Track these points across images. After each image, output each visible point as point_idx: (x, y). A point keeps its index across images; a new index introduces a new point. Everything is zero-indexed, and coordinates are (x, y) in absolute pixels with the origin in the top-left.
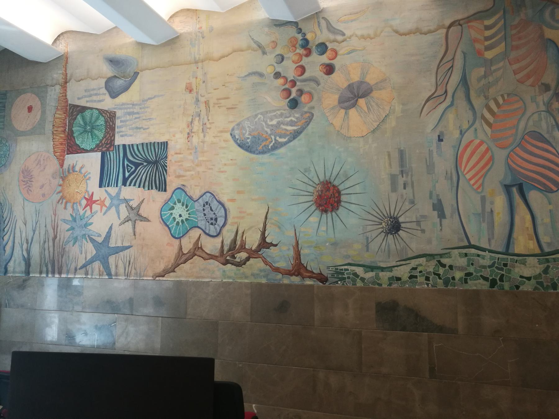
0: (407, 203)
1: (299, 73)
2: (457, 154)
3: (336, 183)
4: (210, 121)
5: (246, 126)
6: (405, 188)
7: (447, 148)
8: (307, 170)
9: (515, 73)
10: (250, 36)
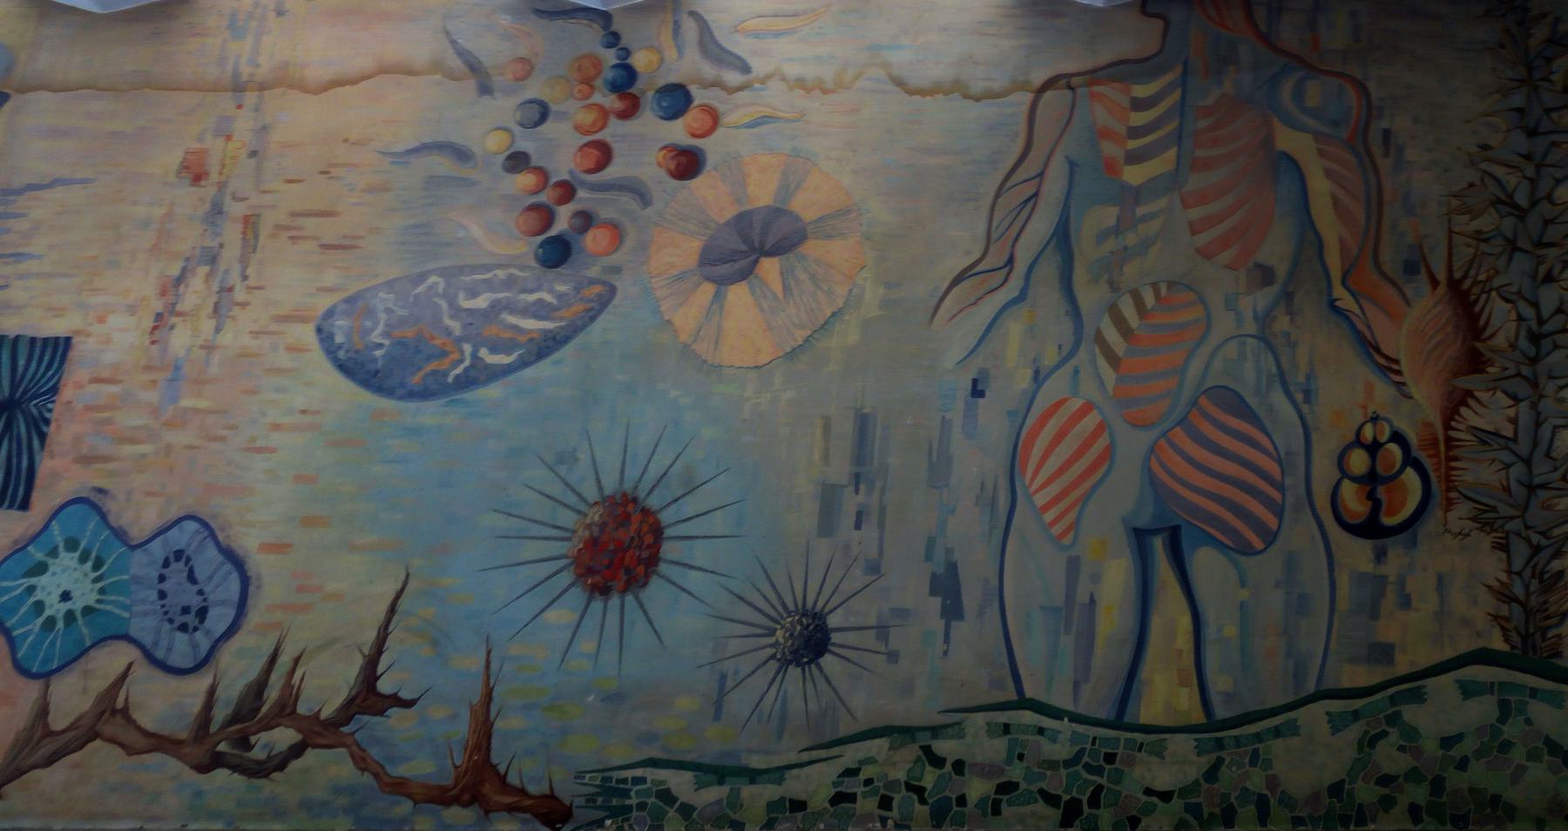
0: (857, 571)
1: (591, 164)
2: (1018, 435)
3: (653, 502)
4: (252, 282)
5: (380, 306)
6: (858, 526)
7: (993, 417)
8: (566, 458)
9: (1194, 229)
10: (447, 33)
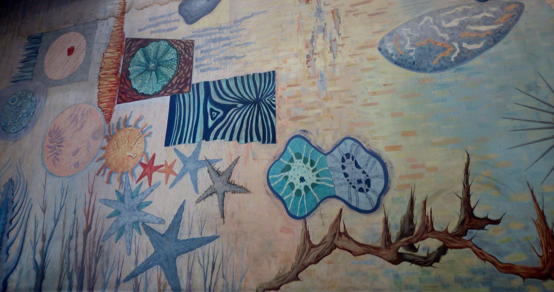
4: (343, 35)
